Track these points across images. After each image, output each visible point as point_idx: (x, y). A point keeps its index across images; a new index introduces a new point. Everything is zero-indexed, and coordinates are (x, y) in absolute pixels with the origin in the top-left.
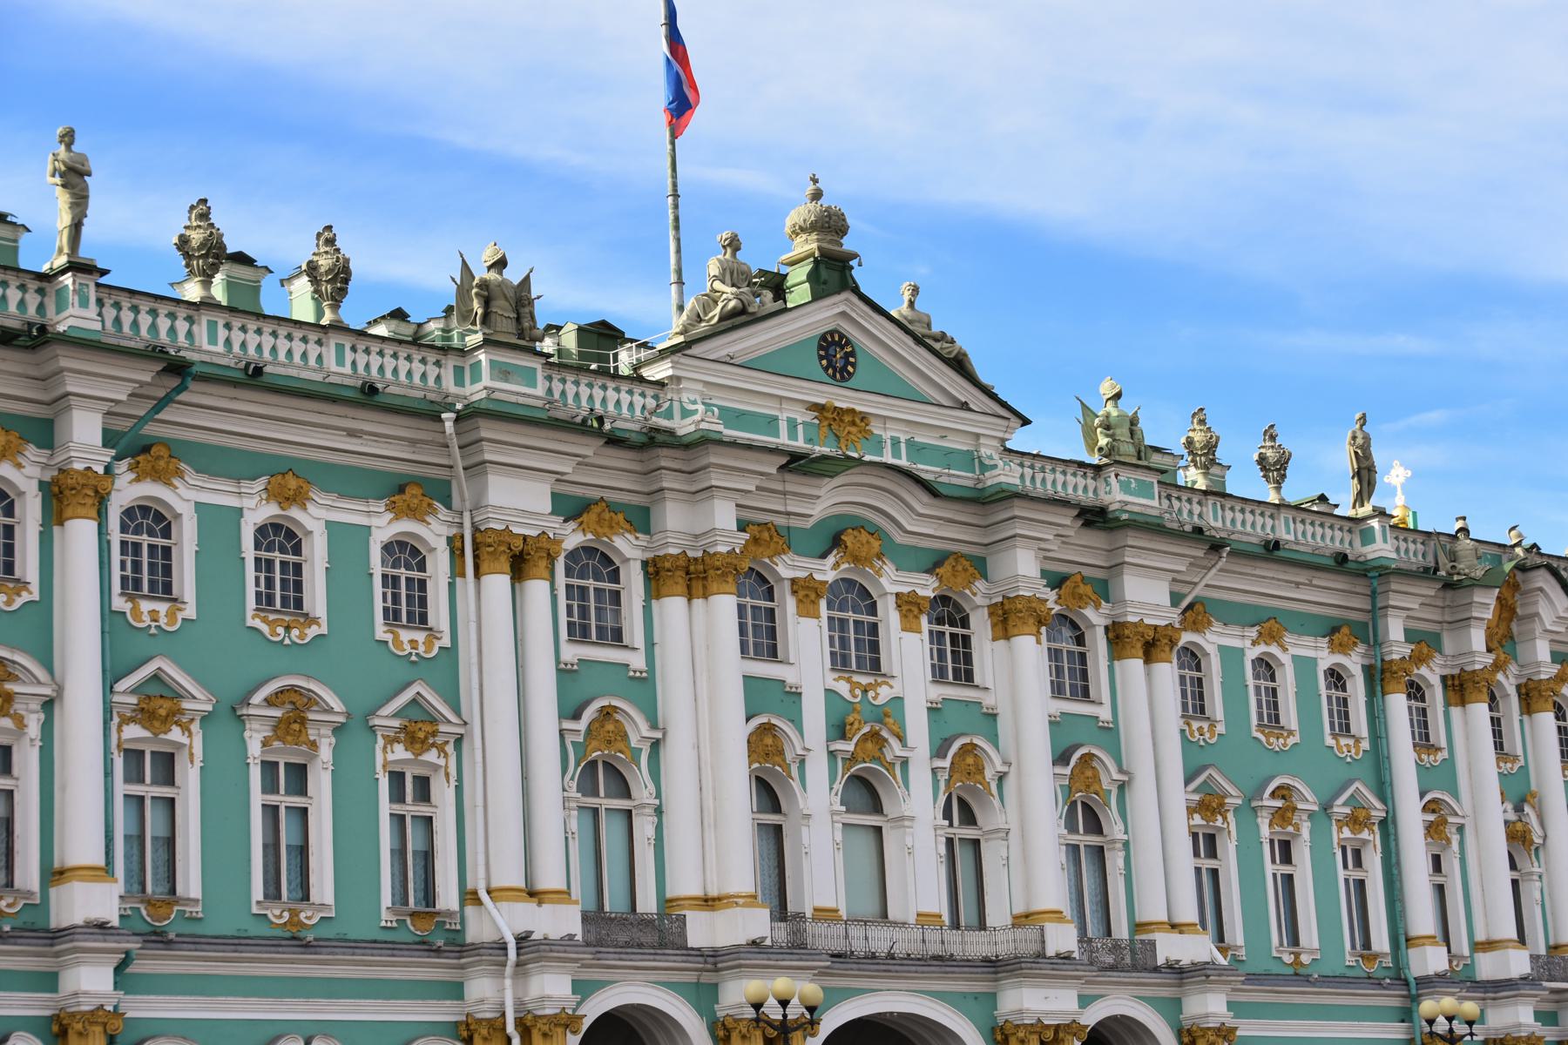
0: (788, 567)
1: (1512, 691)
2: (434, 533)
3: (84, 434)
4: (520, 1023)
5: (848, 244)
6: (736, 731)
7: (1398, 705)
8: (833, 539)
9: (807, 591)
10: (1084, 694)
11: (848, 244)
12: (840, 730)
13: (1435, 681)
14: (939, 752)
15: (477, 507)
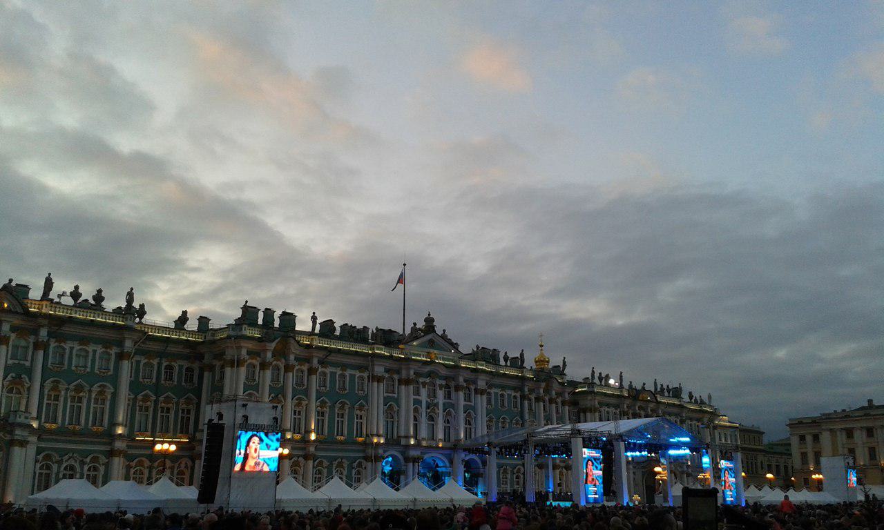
0: (421, 380)
1: (547, 399)
2: (365, 375)
3: (315, 361)
4: (375, 457)
5: (434, 324)
6: (412, 407)
7: (526, 403)
8: (429, 375)
9: (424, 384)
10: (470, 402)
11: (434, 324)
12: (428, 407)
13: (533, 398)
14: (444, 411)
15: (373, 370)
